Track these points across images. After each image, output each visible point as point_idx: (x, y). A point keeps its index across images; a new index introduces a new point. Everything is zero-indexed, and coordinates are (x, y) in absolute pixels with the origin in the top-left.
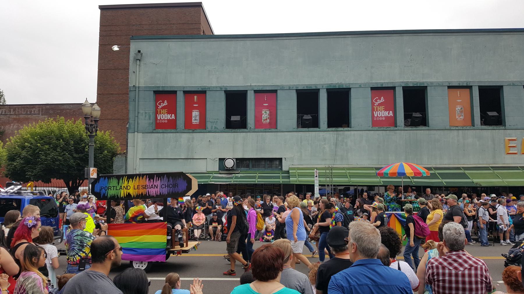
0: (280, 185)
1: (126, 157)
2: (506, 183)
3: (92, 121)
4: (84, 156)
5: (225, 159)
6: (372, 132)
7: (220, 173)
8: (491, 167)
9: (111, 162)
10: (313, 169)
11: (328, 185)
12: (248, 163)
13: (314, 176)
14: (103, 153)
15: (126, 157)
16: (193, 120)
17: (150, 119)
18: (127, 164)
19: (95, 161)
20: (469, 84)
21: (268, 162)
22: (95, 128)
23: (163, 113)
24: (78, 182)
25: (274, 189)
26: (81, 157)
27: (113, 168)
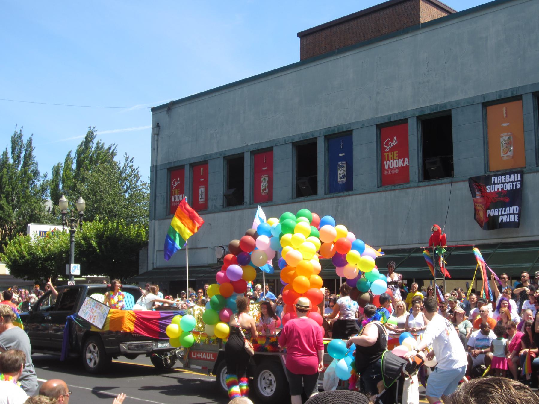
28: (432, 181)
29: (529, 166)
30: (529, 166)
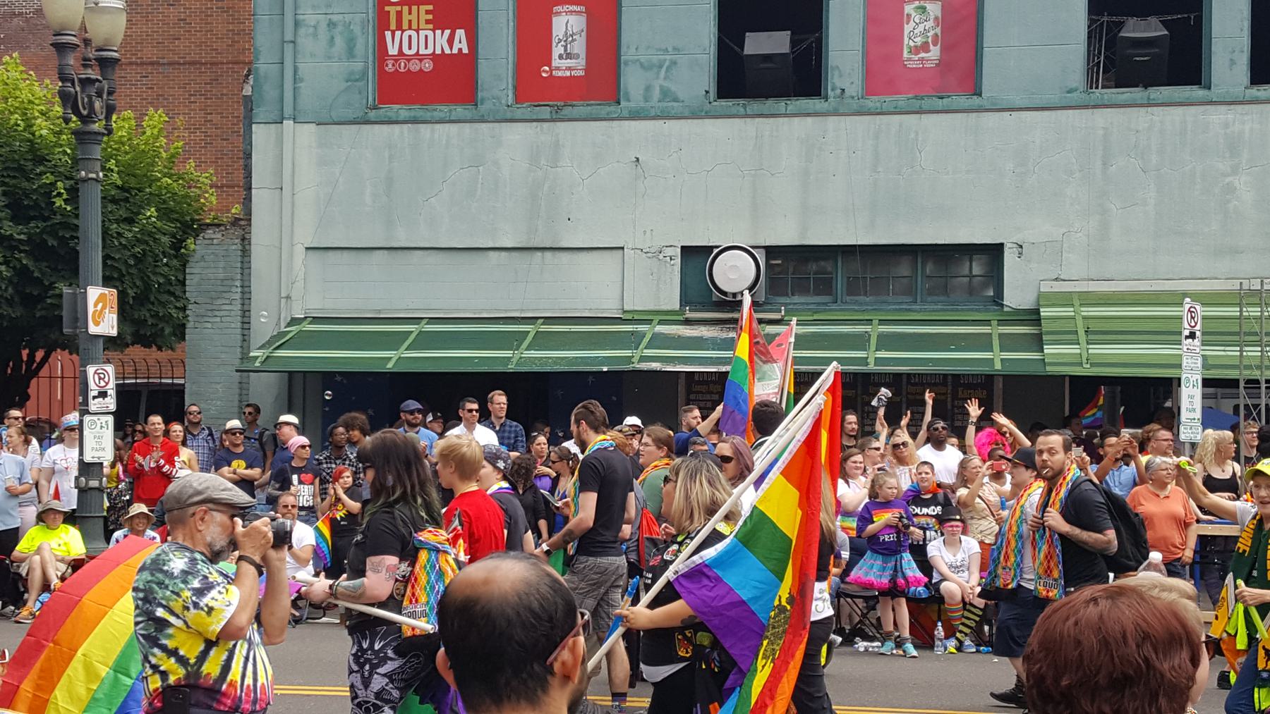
0: (990, 378)
1: (245, 240)
3: (86, 63)
4: (53, 231)
5: (711, 248)
7: (688, 322)
9: (175, 262)
12: (831, 273)
14: (141, 217)
15: (243, 239)
16: (555, 55)
17: (350, 53)
18: (250, 274)
19: (106, 257)
21: (929, 268)
22: (105, 97)
23: (414, 26)
24: (25, 358)
25: (956, 402)
26: (36, 234)
27: (185, 292)
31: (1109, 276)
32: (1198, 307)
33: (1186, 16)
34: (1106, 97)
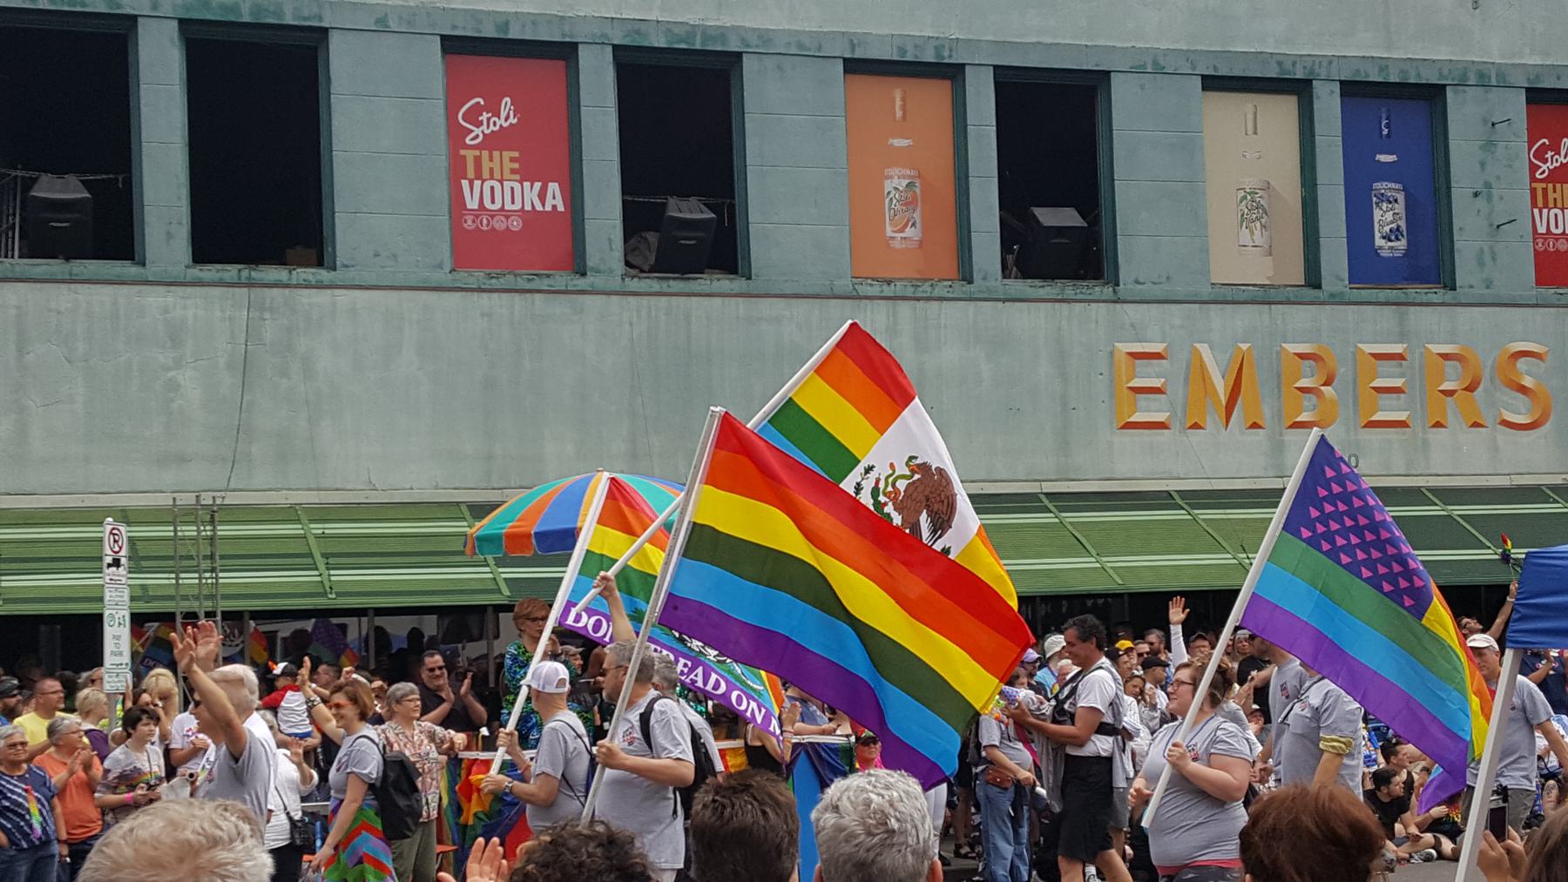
2: (1115, 577)
6: (458, 295)
8: (1047, 494)
10: (93, 517)
11: (191, 617)
13: (100, 559)
20: (950, 56)
28: (674, 279)
29: (984, 279)
30: (984, 279)
31: (28, 490)
32: (122, 529)
33: (111, 176)
34: (17, 268)
